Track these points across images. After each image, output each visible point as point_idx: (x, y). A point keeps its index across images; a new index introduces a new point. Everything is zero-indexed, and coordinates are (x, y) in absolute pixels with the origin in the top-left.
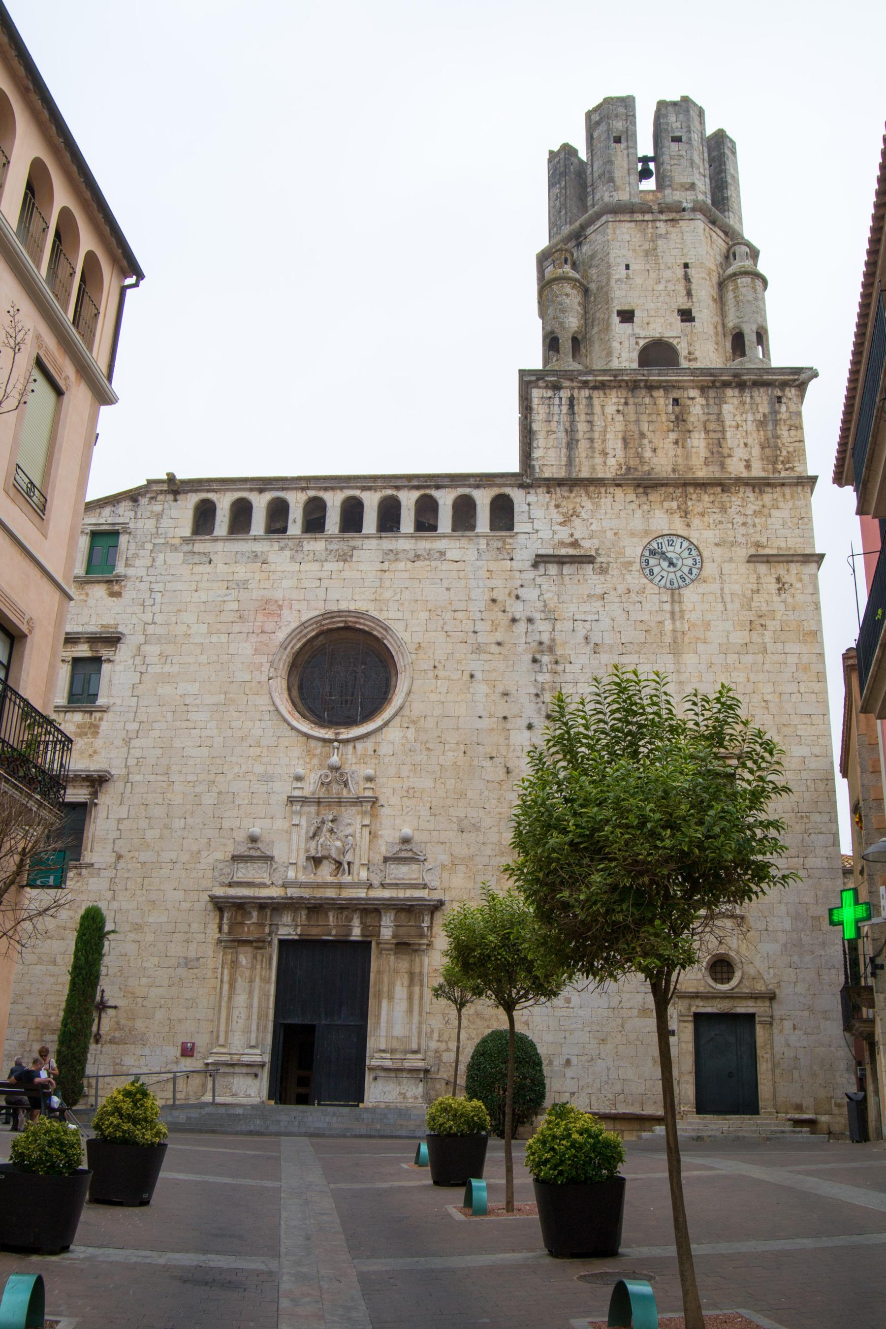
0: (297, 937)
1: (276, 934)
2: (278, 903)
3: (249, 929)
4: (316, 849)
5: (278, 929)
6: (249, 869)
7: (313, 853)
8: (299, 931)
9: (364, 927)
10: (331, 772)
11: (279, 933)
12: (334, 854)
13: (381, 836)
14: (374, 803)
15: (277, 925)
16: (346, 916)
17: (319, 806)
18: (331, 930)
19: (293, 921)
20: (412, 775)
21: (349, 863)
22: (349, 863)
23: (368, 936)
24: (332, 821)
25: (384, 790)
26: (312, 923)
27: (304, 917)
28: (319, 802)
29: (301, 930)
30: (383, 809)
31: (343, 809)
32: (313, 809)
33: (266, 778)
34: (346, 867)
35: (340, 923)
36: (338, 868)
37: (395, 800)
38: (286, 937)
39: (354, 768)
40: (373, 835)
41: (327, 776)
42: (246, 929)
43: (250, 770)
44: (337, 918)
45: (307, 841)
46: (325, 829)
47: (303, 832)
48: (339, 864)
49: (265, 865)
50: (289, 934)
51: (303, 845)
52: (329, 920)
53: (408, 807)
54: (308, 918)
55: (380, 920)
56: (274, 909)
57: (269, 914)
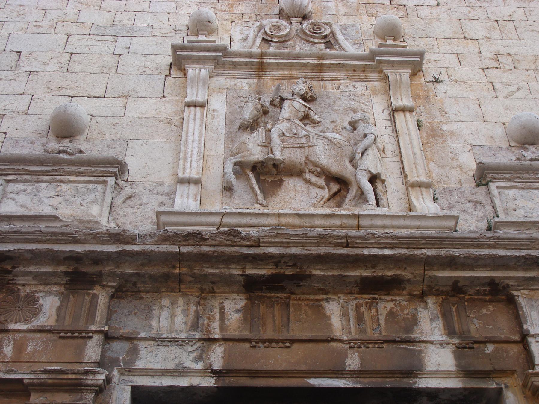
0: (209, 382)
1: (129, 370)
2: (147, 257)
3: (19, 348)
4: (268, 146)
5: (134, 352)
6: (43, 194)
7: (256, 154)
8: (217, 358)
9: (466, 348)
10: (291, 23)
11: (140, 364)
12: (323, 156)
13: (452, 134)
14: (416, 70)
15: (130, 339)
16: (391, 314)
17: (260, 77)
18: (343, 356)
19: (195, 327)
20: (496, 34)
21: (374, 179)
22: (374, 179)
23: (486, 375)
24: (304, 98)
25: (435, 57)
26: (269, 334)
27: (234, 318)
28: (261, 67)
29: (227, 357)
30: (440, 88)
31: (329, 85)
32: (245, 83)
33: (113, 32)
34: (368, 187)
35: (371, 334)
36: (337, 197)
37: (470, 72)
38: (167, 382)
39: (344, 20)
40: (432, 134)
41: (278, 28)
42: (8, 350)
43: (72, 16)
44: (360, 319)
45: (230, 138)
46: (286, 110)
47: (220, 121)
48: (339, 185)
49: (99, 187)
50: (180, 371)
51: (219, 147)
52: (329, 326)
53: (509, 84)
54: (249, 315)
55: (518, 319)
56: (125, 290)
57: (102, 300)
